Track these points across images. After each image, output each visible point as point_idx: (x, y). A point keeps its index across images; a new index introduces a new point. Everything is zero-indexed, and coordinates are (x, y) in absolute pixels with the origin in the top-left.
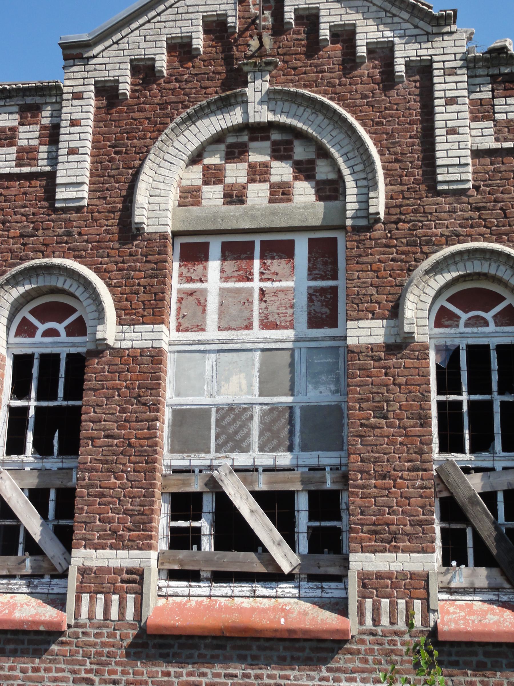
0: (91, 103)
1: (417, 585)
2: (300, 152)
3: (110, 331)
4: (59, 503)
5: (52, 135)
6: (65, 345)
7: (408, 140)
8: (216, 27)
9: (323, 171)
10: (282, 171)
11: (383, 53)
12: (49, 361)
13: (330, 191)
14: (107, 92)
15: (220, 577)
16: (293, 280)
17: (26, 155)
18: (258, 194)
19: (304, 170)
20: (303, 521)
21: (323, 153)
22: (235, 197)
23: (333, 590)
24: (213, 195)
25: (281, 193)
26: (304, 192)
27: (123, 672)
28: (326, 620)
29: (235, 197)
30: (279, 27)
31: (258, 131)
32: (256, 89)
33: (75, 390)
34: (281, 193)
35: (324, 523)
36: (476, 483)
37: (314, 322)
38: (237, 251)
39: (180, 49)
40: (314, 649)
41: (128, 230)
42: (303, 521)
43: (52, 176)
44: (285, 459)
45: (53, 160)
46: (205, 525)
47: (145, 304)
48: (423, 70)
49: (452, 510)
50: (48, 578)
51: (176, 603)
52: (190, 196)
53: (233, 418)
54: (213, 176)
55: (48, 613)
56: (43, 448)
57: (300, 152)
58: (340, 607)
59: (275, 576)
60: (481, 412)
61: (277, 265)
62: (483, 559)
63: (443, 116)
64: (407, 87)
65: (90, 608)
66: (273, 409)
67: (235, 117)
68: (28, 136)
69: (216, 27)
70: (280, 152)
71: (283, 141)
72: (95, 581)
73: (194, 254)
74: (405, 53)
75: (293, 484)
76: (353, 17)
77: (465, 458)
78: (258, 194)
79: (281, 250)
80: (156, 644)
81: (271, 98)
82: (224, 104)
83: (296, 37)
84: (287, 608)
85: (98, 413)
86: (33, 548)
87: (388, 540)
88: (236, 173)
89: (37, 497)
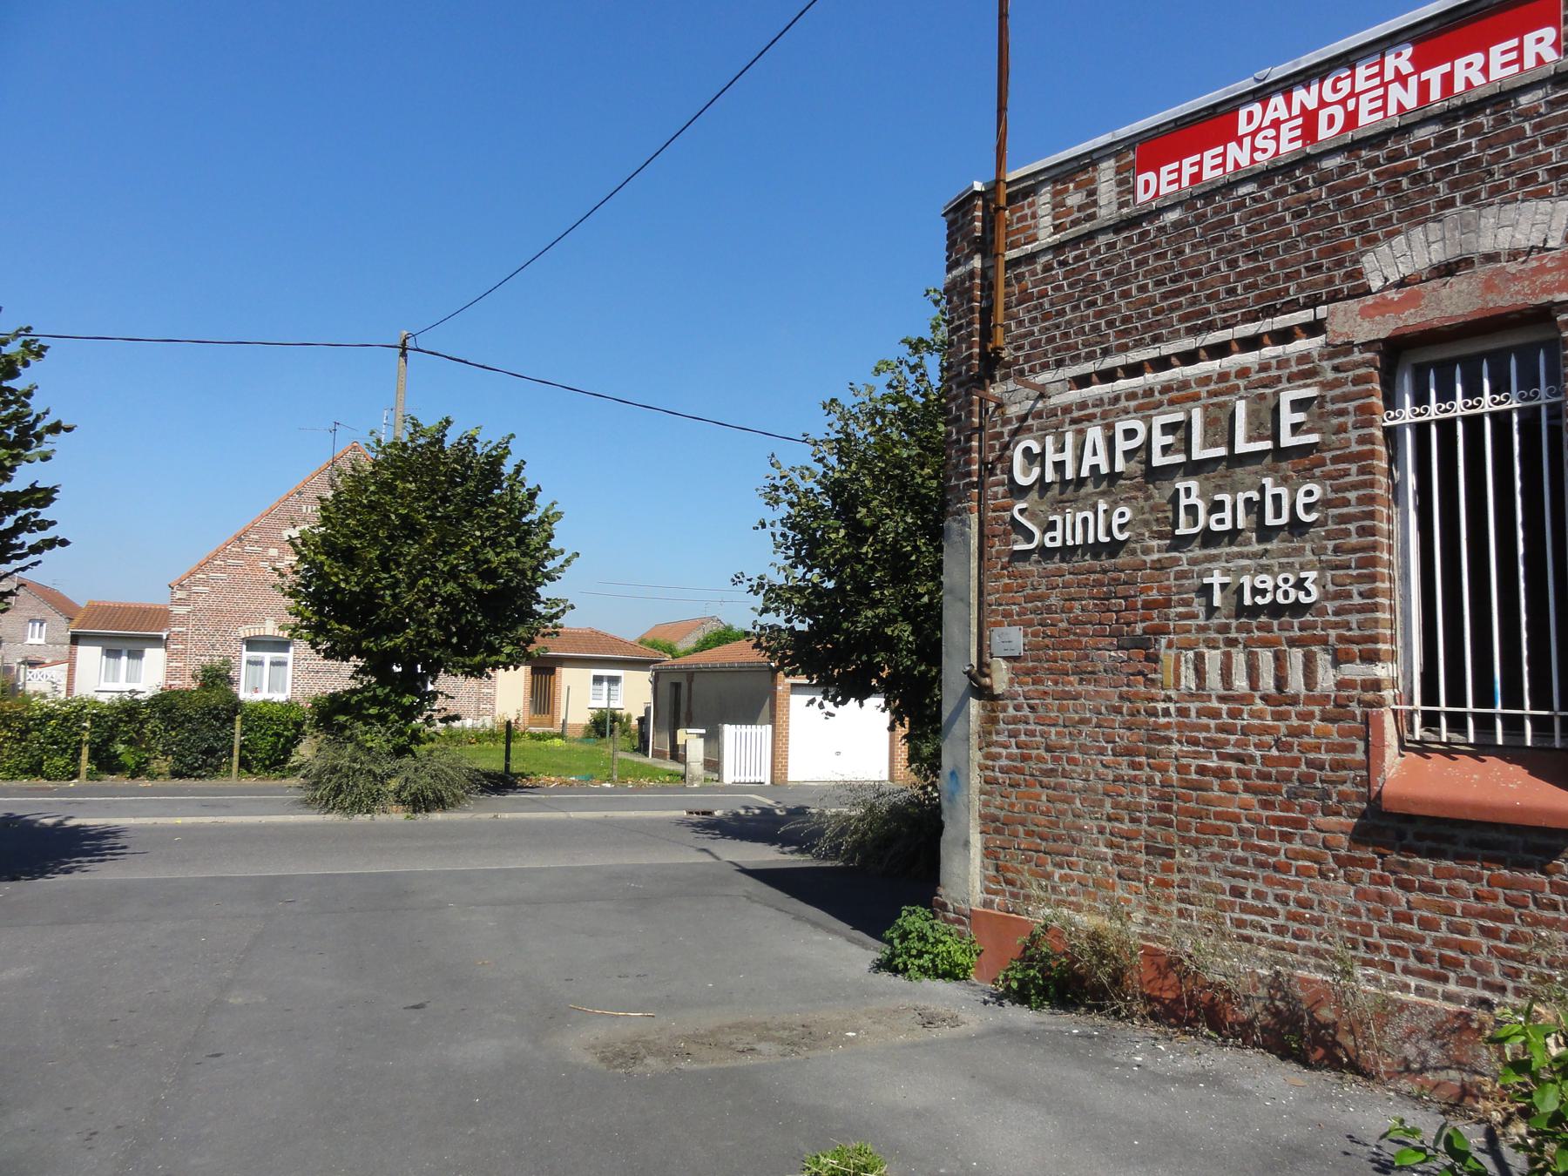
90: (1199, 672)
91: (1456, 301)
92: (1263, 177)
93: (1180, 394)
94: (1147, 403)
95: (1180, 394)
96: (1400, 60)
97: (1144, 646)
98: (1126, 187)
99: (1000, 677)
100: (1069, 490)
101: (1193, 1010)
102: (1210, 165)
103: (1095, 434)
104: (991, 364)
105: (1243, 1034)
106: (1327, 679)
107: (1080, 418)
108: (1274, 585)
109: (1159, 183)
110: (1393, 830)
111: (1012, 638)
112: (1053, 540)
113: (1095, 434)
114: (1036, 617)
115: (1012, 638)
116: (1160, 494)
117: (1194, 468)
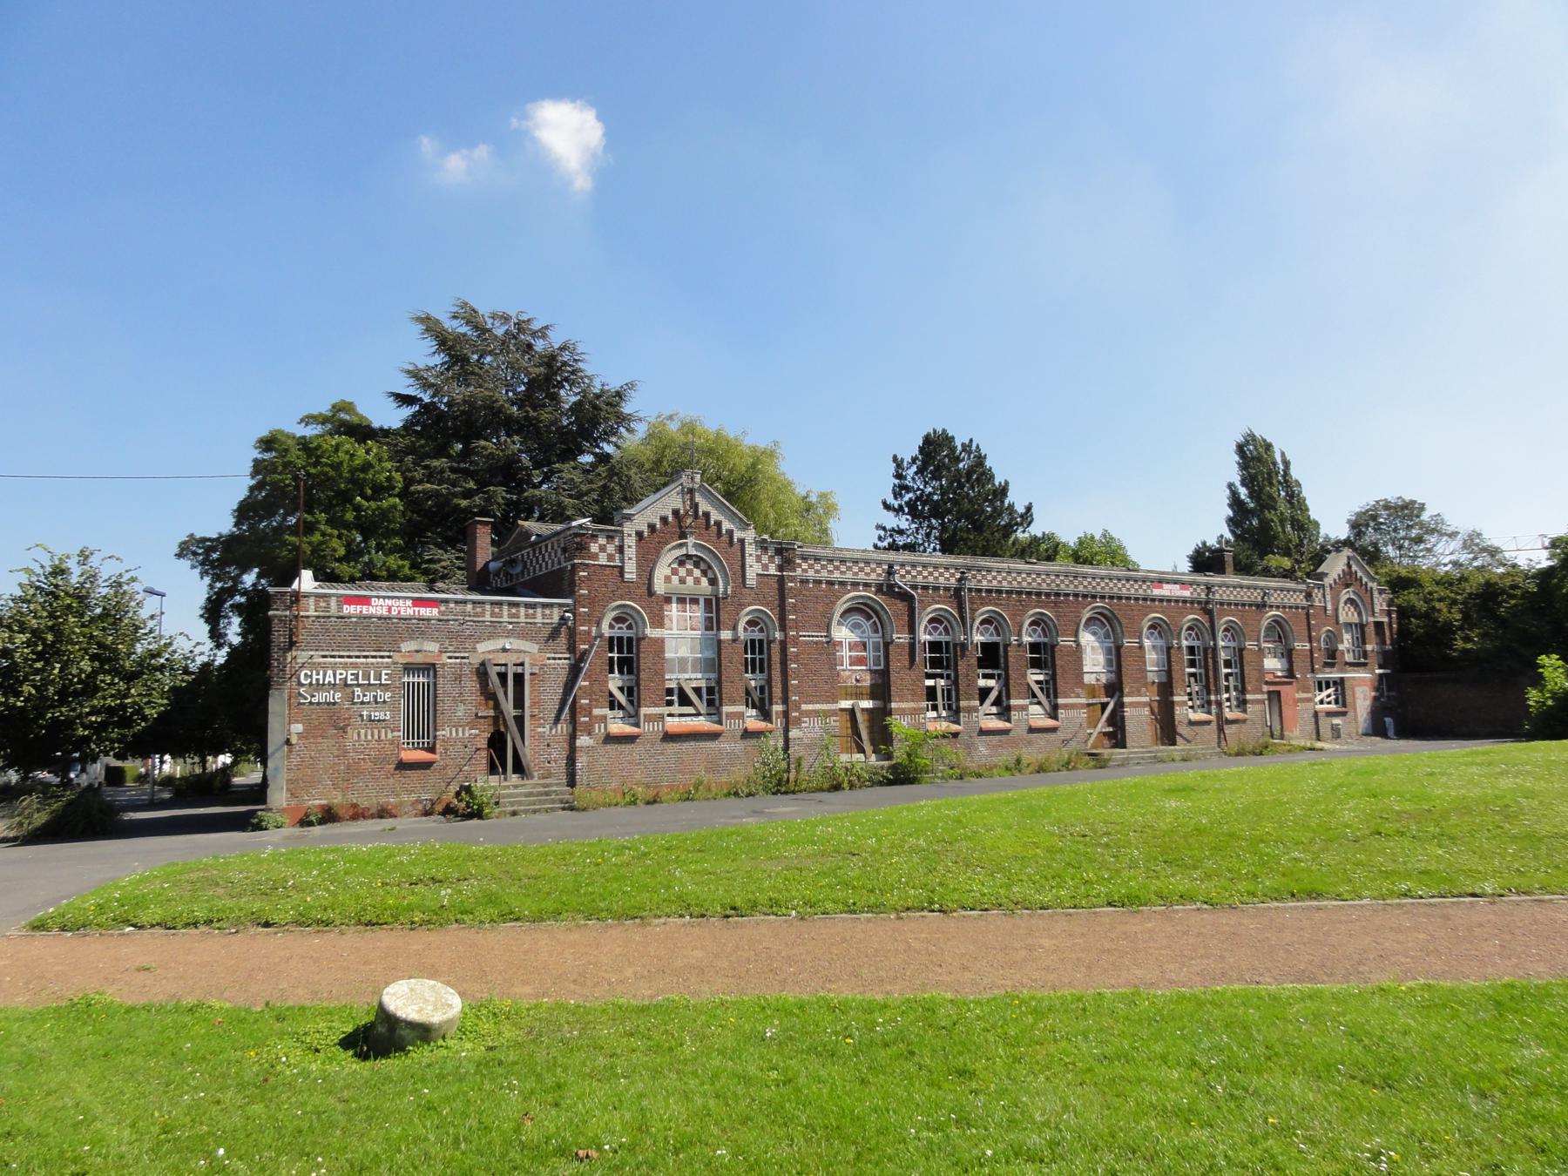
0: (634, 538)
1: (741, 716)
2: (703, 566)
3: (649, 631)
4: (630, 692)
5: (621, 550)
6: (626, 633)
7: (737, 567)
8: (676, 513)
9: (710, 575)
10: (697, 572)
11: (730, 533)
12: (620, 639)
13: (713, 582)
14: (639, 534)
15: (681, 715)
16: (698, 613)
17: (611, 558)
18: (690, 580)
19: (704, 573)
20: (705, 696)
21: (710, 567)
22: (682, 581)
23: (715, 718)
24: (675, 579)
25: (697, 581)
26: (704, 581)
27: (660, 747)
28: (716, 727)
29: (682, 581)
30: (696, 516)
31: (689, 557)
32: (691, 540)
33: (630, 651)
34: (697, 581)
35: (713, 698)
36: (753, 683)
37: (707, 629)
38: (681, 601)
39: (664, 520)
40: (713, 736)
41: (651, 593)
42: (705, 696)
43: (621, 569)
44: (699, 676)
45: (622, 561)
46: (675, 698)
47: (659, 622)
48: (742, 541)
49: (748, 693)
50: (633, 718)
51: (674, 724)
52: (668, 579)
53: (682, 664)
54: (675, 572)
55: (635, 730)
56: (621, 672)
57: (703, 566)
58: (720, 722)
59: (699, 714)
60: (753, 660)
61: (695, 607)
62: (754, 707)
63: (749, 560)
64: (737, 546)
65: (646, 727)
66: (696, 659)
67: (683, 551)
68: (611, 549)
69: (676, 513)
70: (696, 565)
71: (698, 562)
72: (649, 718)
73: (668, 600)
74: (737, 535)
75: (703, 684)
76: (721, 518)
77: (749, 675)
78: (690, 580)
79: (695, 601)
80: (669, 737)
81: (696, 545)
82: (681, 546)
83: (702, 521)
84: (702, 723)
85: (646, 662)
86: (621, 707)
87: (733, 702)
88: (682, 571)
89: (621, 689)
90: (357, 736)
91: (419, 658)
92: (380, 618)
93: (355, 666)
94: (345, 667)
95: (355, 666)
96: (409, 603)
97: (344, 729)
98: (340, 608)
99: (294, 740)
100: (320, 686)
101: (358, 814)
102: (365, 610)
103: (330, 672)
104: (292, 644)
105: (372, 817)
106: (390, 736)
107: (325, 667)
108: (377, 715)
109: (349, 609)
110: (402, 766)
111: (298, 728)
112: (315, 700)
113: (330, 672)
114: (307, 722)
115: (298, 728)
116: (349, 690)
117: (358, 685)
